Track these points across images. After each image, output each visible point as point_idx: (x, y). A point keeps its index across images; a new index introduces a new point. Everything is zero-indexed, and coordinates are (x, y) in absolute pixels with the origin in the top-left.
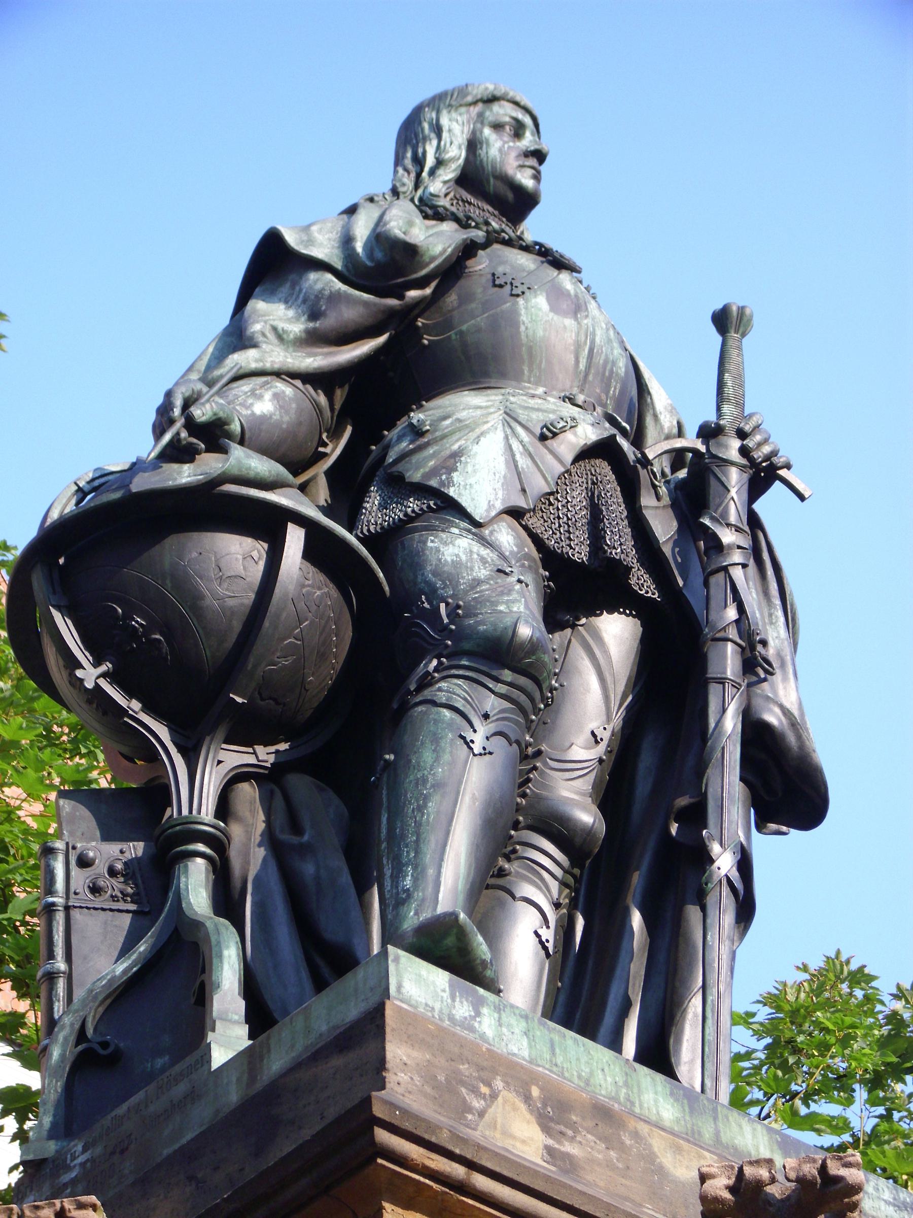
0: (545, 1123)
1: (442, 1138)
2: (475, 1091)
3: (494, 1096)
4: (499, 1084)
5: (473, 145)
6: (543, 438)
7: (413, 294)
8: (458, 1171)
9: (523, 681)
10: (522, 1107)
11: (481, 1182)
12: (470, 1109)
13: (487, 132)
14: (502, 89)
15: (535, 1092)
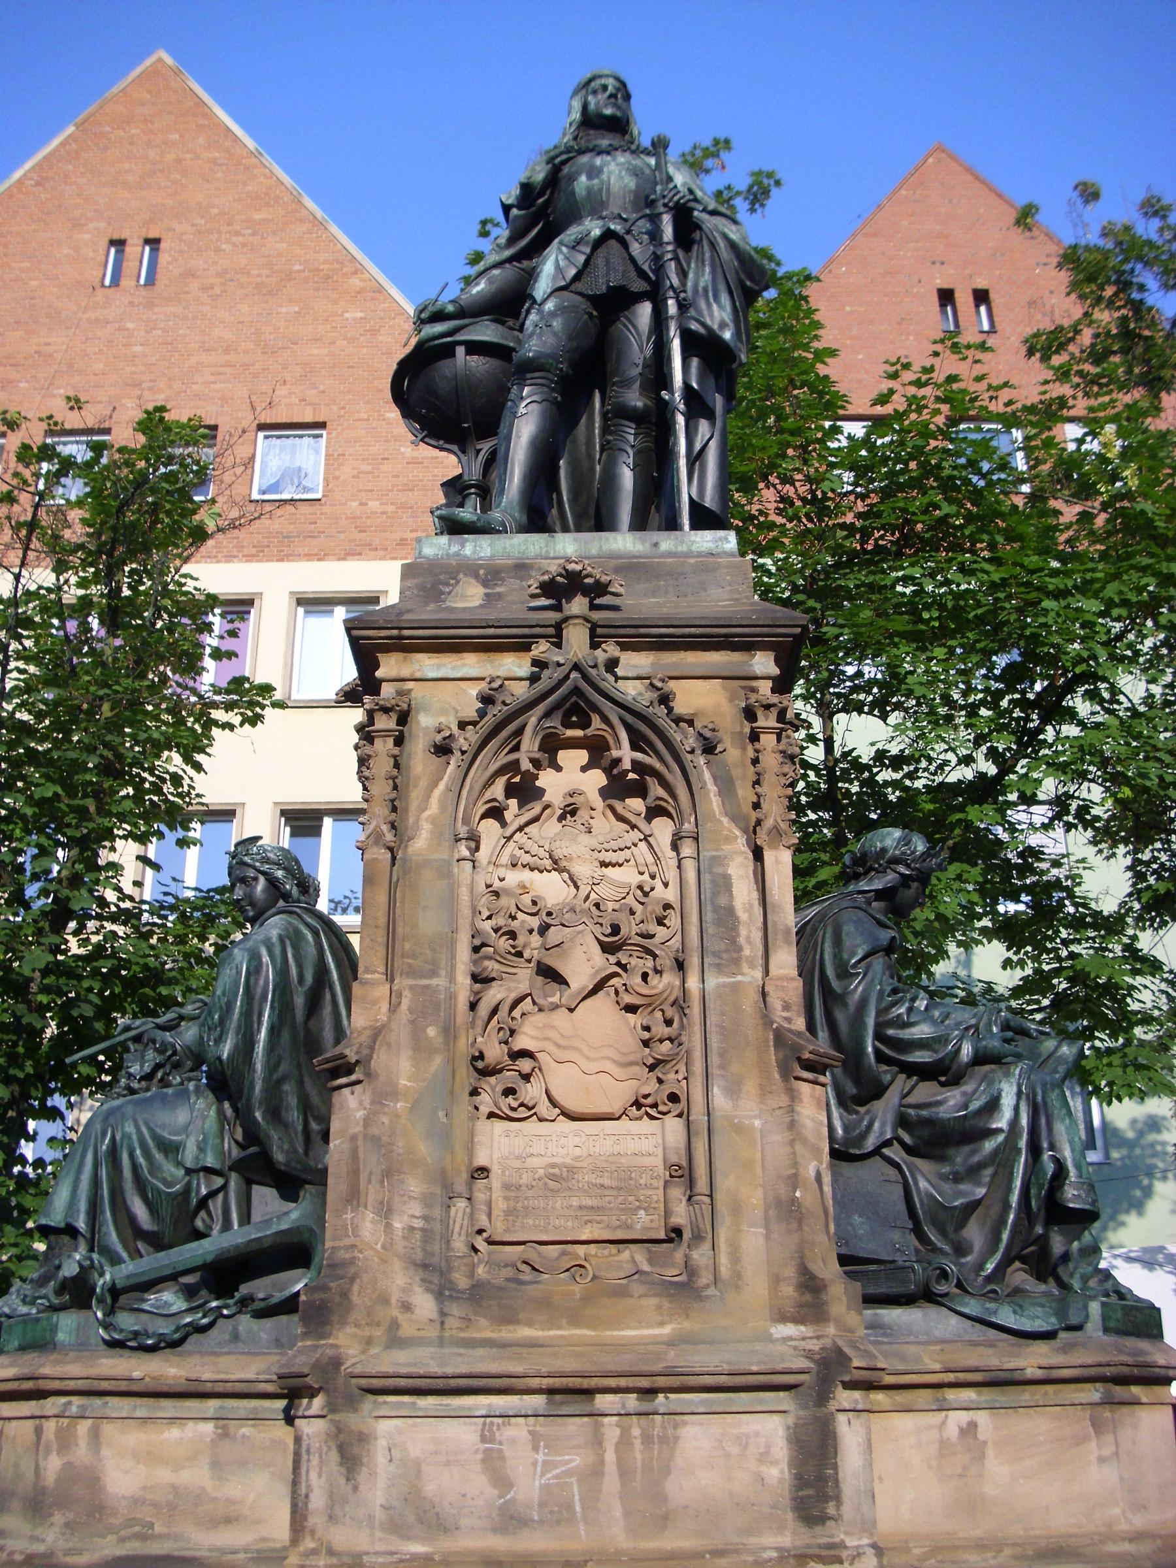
0: (485, 584)
1: (381, 623)
2: (448, 585)
3: (458, 582)
4: (461, 576)
5: (585, 107)
6: (573, 248)
7: (541, 201)
8: (395, 632)
9: (537, 374)
10: (473, 581)
11: (406, 633)
12: (442, 593)
13: (590, 98)
14: (596, 72)
15: (482, 572)
